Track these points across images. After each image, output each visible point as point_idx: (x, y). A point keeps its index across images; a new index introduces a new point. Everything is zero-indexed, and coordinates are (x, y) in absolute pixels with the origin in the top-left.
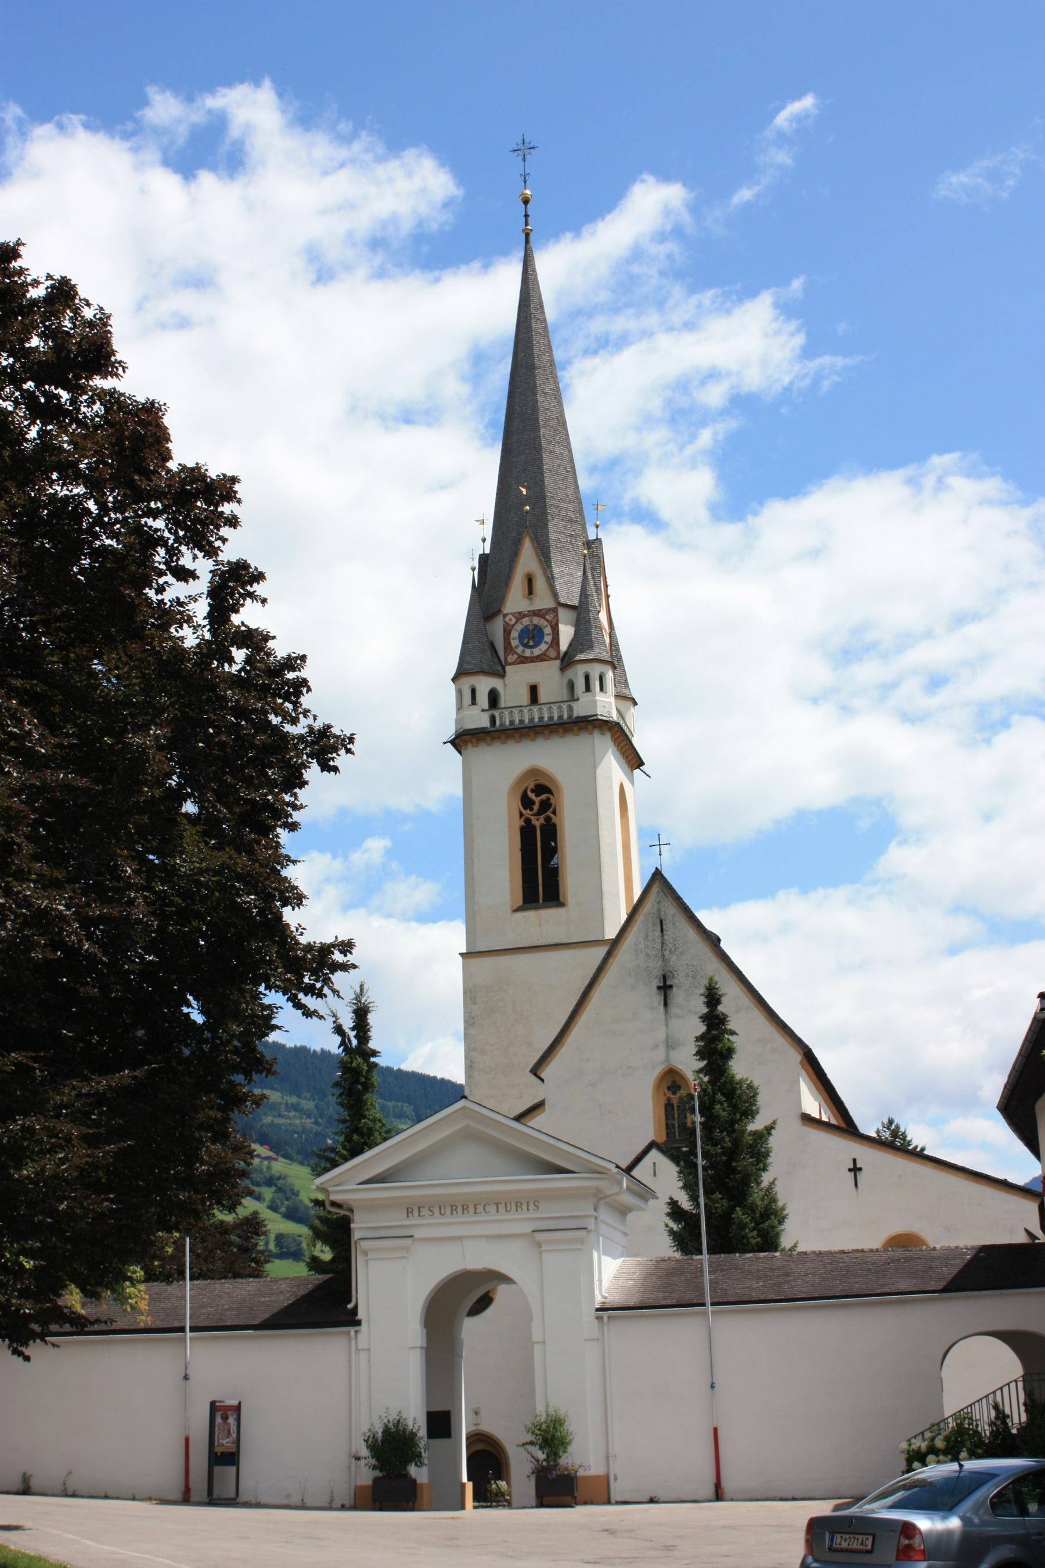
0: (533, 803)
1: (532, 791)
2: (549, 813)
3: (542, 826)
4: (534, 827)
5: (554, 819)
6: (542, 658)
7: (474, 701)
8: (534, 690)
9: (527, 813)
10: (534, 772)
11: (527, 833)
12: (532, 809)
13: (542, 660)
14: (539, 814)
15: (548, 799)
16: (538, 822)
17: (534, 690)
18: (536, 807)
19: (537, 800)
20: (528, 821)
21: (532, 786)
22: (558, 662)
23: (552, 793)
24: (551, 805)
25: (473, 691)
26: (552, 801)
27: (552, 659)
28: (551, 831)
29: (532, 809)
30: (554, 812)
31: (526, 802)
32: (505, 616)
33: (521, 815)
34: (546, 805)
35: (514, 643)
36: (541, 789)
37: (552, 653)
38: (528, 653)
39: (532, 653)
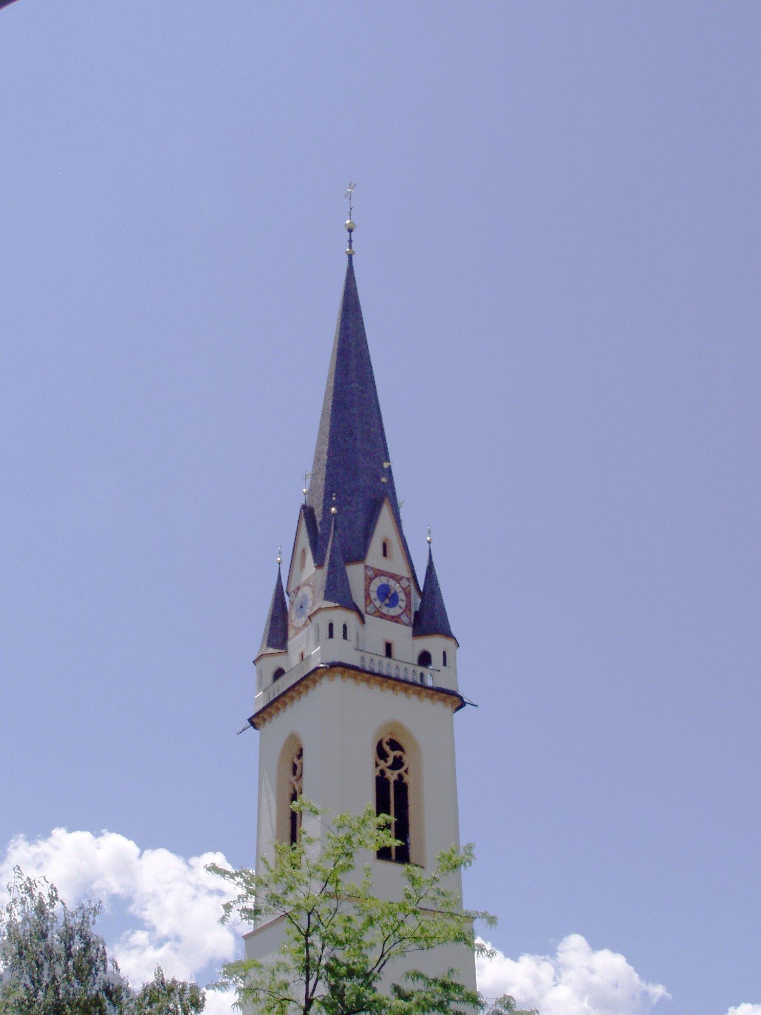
0: (388, 756)
1: (388, 743)
2: (402, 770)
3: (395, 781)
4: (387, 782)
5: (406, 779)
6: (395, 619)
7: (345, 637)
8: (388, 648)
9: (382, 762)
10: (396, 725)
11: (381, 783)
12: (386, 761)
13: (396, 622)
14: (393, 767)
15: (401, 758)
16: (392, 776)
17: (388, 648)
18: (390, 761)
19: (392, 754)
20: (382, 772)
21: (387, 739)
22: (409, 630)
23: (404, 752)
24: (401, 765)
25: (345, 627)
26: (406, 759)
27: (405, 624)
28: (402, 788)
29: (386, 761)
30: (406, 771)
31: (381, 753)
32: (366, 567)
33: (377, 765)
34: (398, 764)
35: (374, 595)
36: (395, 745)
37: (404, 618)
38: (385, 610)
39: (388, 611)
